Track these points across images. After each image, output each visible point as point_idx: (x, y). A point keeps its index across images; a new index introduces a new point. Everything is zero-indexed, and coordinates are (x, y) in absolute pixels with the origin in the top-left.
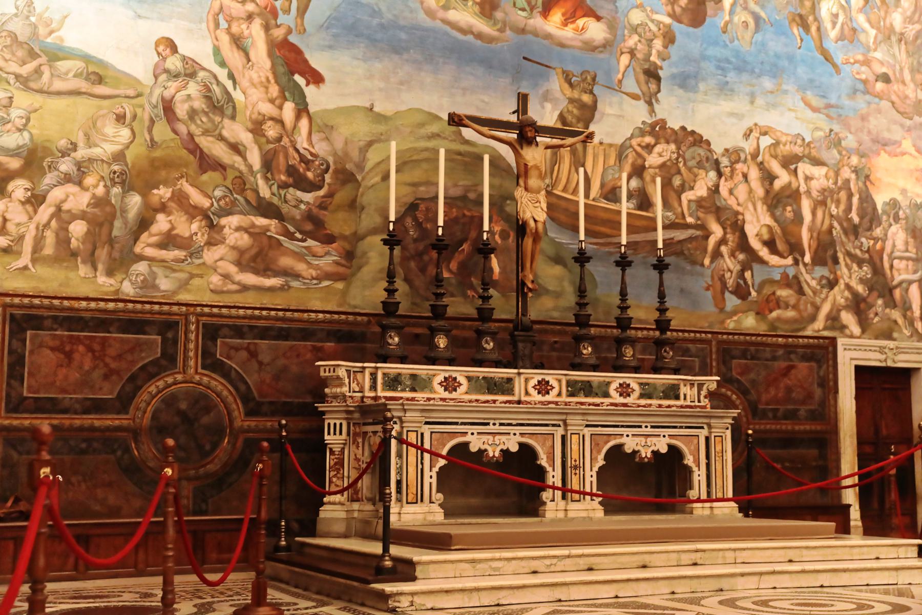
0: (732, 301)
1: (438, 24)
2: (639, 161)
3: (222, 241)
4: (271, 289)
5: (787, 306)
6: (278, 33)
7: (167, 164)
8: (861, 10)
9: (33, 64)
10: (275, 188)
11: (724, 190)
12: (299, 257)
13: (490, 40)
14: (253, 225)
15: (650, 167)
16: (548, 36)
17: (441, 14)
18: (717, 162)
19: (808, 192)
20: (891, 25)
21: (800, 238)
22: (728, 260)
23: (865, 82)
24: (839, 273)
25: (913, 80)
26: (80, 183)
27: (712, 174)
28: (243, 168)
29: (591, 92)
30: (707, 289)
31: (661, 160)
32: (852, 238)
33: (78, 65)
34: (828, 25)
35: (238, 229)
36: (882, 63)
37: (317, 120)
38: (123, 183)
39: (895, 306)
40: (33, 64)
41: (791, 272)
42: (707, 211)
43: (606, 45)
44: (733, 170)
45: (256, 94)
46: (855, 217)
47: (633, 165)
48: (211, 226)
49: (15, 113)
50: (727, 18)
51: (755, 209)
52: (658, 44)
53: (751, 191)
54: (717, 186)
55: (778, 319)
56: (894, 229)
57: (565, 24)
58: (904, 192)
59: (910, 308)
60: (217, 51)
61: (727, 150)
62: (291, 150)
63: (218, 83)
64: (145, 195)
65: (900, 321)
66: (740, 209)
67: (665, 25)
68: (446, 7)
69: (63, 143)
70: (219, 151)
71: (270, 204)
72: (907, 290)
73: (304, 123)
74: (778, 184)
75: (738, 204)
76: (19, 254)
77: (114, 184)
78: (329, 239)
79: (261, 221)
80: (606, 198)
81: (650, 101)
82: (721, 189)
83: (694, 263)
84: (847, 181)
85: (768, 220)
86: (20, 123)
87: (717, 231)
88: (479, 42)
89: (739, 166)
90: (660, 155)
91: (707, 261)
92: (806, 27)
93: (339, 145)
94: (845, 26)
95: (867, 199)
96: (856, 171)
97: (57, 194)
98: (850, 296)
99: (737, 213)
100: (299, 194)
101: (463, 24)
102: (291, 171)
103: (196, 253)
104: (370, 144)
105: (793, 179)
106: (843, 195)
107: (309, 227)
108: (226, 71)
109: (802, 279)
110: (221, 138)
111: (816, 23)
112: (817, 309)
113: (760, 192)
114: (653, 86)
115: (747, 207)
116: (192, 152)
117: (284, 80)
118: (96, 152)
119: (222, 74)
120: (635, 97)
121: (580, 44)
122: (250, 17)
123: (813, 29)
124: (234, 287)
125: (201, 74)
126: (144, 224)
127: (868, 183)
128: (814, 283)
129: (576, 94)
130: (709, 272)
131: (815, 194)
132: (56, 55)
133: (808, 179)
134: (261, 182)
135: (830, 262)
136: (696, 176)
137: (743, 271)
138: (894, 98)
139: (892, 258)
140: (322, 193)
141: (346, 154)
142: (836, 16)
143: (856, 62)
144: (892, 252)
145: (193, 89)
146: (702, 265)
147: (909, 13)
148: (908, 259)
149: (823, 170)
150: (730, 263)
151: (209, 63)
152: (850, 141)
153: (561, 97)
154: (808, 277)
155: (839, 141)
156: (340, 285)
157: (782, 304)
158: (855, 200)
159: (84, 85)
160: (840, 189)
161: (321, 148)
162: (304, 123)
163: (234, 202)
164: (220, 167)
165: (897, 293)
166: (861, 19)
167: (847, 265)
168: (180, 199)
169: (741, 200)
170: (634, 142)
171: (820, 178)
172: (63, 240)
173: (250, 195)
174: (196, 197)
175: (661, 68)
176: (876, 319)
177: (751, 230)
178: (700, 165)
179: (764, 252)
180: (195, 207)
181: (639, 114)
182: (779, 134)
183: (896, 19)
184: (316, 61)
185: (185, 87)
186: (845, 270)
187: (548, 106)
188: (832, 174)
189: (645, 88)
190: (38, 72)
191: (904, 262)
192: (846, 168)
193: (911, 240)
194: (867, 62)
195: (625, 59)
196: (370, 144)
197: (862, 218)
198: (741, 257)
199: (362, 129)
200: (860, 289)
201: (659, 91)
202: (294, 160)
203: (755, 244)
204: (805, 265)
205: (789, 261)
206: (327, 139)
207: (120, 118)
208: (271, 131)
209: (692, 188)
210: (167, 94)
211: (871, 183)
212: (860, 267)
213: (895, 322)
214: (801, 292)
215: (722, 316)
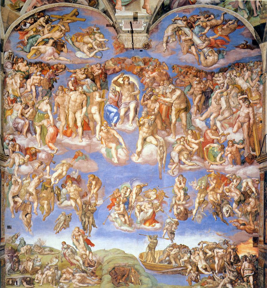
0: (193, 283)
1: (119, 230)
2: (169, 253)
3: (76, 278)
4: (85, 287)
5: (210, 283)
6: (85, 237)
7: (65, 265)
8: (236, 208)
9: (41, 250)
10: (85, 268)
11: (192, 258)
12: (90, 280)
13: (131, 231)
14: (81, 275)
15: (172, 254)
16: (145, 229)
17: (120, 228)
18: (190, 251)
19: (217, 256)
20: (247, 210)
21: (215, 267)
22: (193, 274)
23: (237, 226)
24: (226, 275)
25: (253, 224)
26: (50, 270)
27: (189, 254)
28: (79, 264)
29: (156, 239)
30: (187, 281)
31: (175, 252)
32: (231, 266)
33: (49, 249)
34: (226, 214)
35: (78, 276)
36: (243, 221)
37: (93, 253)
38: (57, 269)
39: (244, 282)
40: (41, 250)
41: (211, 276)
42: (187, 263)
43: (160, 228)
44: (194, 253)
45: (81, 250)
46: (232, 261)
47: (167, 254)
48: (73, 275)
49: (38, 259)
50: (194, 217)
51: (201, 261)
52: (174, 226)
53: (200, 257)
54: (190, 258)
55: (207, 287)
56: (245, 263)
57: (150, 225)
58: (249, 253)
59: (249, 282)
60: (73, 243)
61: (193, 248)
62: (88, 260)
63: (74, 248)
64: (61, 271)
65: (246, 285)
66: (197, 262)
67: (176, 221)
68: (121, 226)
69: (47, 263)
70: (74, 261)
71: (84, 271)
72: (248, 278)
73: (91, 254)
74: (208, 255)
75: (196, 261)
76: (40, 283)
77: (55, 269)
78: (97, 276)
79: (83, 274)
80: (160, 263)
81: (172, 239)
82: (191, 257)
83: (183, 275)
84: (230, 252)
85: (205, 264)
86: (39, 260)
87: (190, 267)
88: (128, 233)
89: (197, 252)
90: (174, 252)
91: (187, 275)
92: (217, 215)
93: (98, 257)
94: (231, 213)
95: (236, 256)
96: (233, 249)
97: (46, 272)
98: (229, 280)
99: (196, 263)
100: (90, 268)
101: (125, 229)
102: (88, 264)
103: (71, 281)
104: (104, 257)
105: (213, 253)
106: (228, 256)
107: (92, 274)
108: (75, 246)
109: (215, 277)
110: (75, 259)
111: (221, 214)
112: (219, 284)
113: (202, 257)
114: (173, 236)
115: (199, 261)
116: (69, 262)
117: (86, 247)
118: (52, 264)
119: (74, 247)
120: (167, 239)
121: (153, 229)
122: (79, 235)
123: (220, 215)
124: (78, 287)
125: (71, 248)
126: (61, 276)
127: (237, 252)
128: (218, 278)
129: (152, 240)
130: (187, 277)
131: (219, 256)
132: (45, 248)
133: (217, 253)
134: (83, 267)
135: (223, 273)
136: (184, 255)
137: (197, 276)
138: (246, 229)
139: (244, 270)
140: (95, 267)
141: (100, 259)
142: (228, 211)
143: (235, 221)
144: (244, 268)
145: (69, 250)
146: (186, 275)
147: (253, 206)
148: (249, 270)
149: (222, 250)
150: (193, 275)
151: (72, 245)
152: (231, 242)
153: (148, 242)
154: (216, 276)
155: (228, 243)
156: (99, 285)
157: (208, 283)
158: (232, 257)
159: (50, 253)
160: (228, 254)
161: (94, 259)
162: (91, 254)
163: (78, 271)
164: (75, 264)
165: (245, 279)
166: (236, 211)
167: (229, 273)
168: (68, 271)
169: (197, 259)
170: (167, 249)
171: (221, 252)
172: (48, 281)
173: (81, 269)
174: (70, 271)
175: (175, 231)
176: (238, 285)
177: (200, 267)
178: (185, 253)
179: (203, 271)
180: (70, 272)
181: (169, 243)
182: (208, 243)
183: (249, 209)
184: (93, 242)
185: (67, 250)
186: (229, 274)
187: (145, 244)
188: (225, 251)
189: (170, 237)
190: (42, 251)
191: (248, 271)
192: (230, 249)
193: (250, 265)
194: (238, 221)
195: (165, 231)
196: (104, 257)
197: (234, 261)
198: (197, 273)
199: (103, 254)
200: (233, 278)
201: (174, 237)
202: (89, 261)
203: (201, 269)
204: (216, 273)
205: (211, 273)
206: (95, 257)
207: (56, 258)
208: (84, 257)
209: (183, 258)
210: (64, 252)
211: (238, 252)
212: (233, 273)
213: (244, 286)
214: (214, 280)
215: (191, 287)
